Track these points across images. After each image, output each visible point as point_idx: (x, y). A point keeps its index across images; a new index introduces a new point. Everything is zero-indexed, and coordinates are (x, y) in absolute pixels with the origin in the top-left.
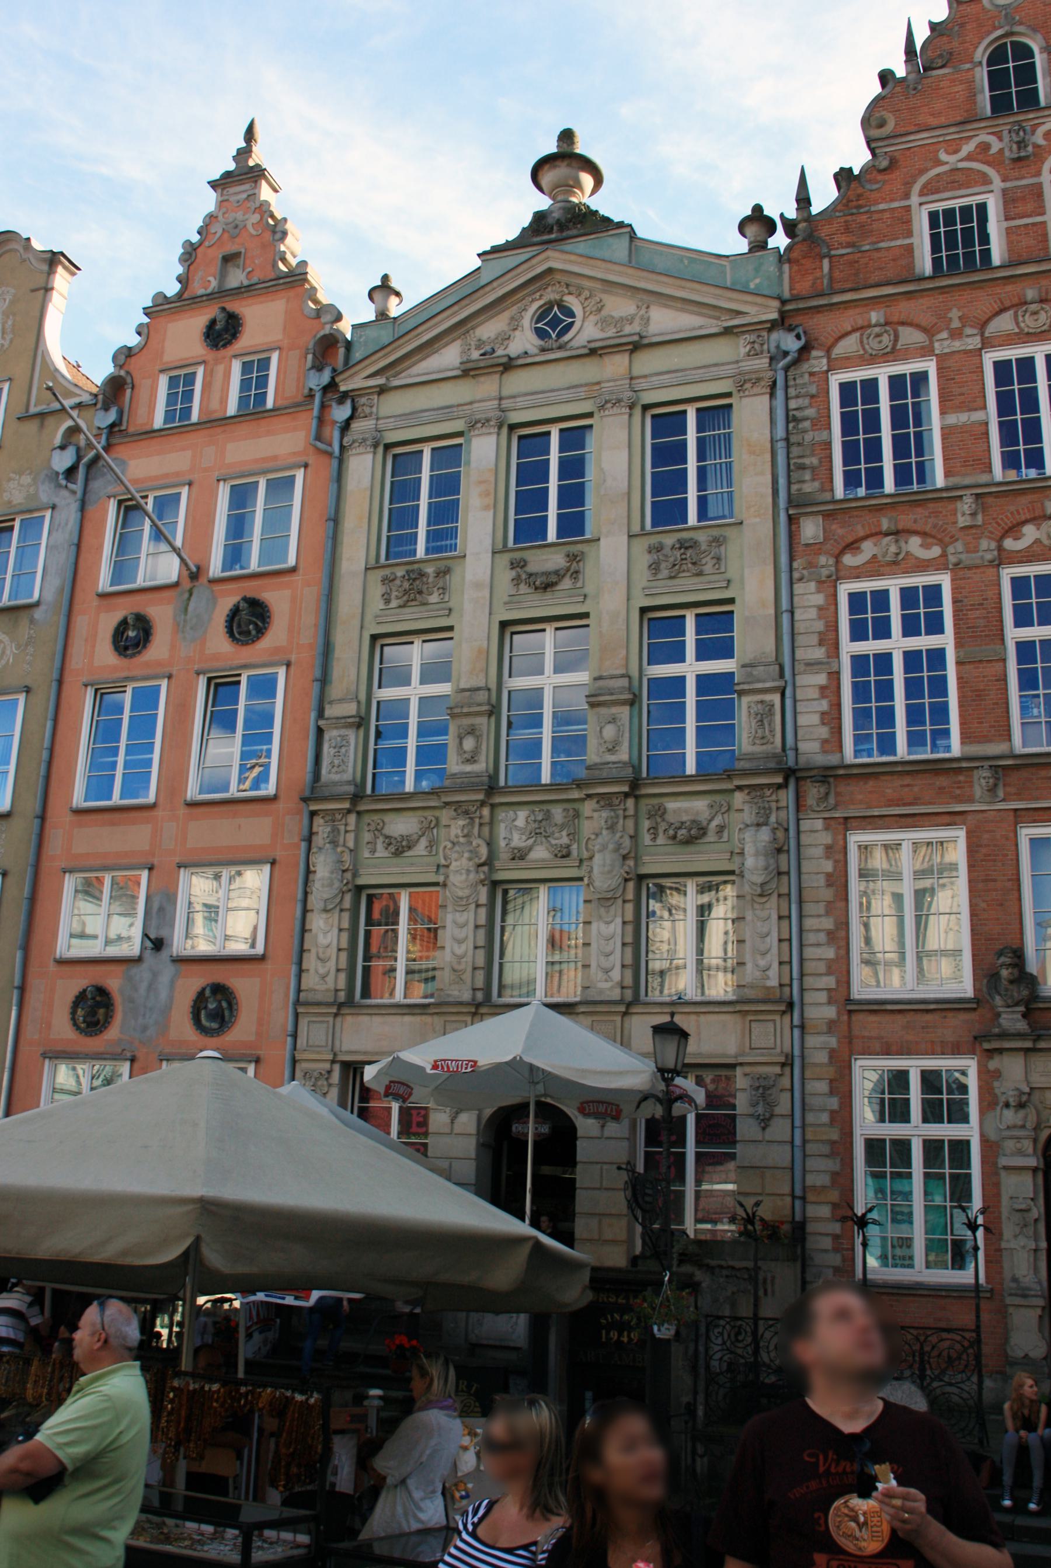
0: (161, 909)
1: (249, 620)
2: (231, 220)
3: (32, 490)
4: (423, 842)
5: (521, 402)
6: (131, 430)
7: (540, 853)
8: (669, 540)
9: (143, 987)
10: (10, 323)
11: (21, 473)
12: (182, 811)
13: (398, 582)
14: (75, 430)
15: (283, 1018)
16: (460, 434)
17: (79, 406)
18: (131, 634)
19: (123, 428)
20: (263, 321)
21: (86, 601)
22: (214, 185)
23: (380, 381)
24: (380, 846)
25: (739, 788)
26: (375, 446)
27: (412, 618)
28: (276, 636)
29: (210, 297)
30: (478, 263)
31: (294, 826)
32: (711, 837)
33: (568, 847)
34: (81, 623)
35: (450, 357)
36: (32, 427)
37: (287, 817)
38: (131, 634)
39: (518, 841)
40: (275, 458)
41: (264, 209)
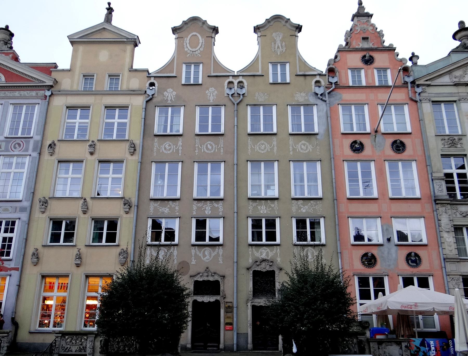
0: (387, 230)
1: (399, 146)
2: (362, 27)
3: (306, 98)
6: (341, 85)
9: (386, 253)
10: (284, 44)
11: (301, 92)
12: (388, 200)
13: (446, 140)
15: (436, 263)
16: (455, 101)
17: (320, 75)
18: (357, 146)
19: (338, 83)
20: (380, 59)
24: (458, 214)
27: (453, 151)
28: (409, 151)
29: (363, 50)
31: (428, 207)
34: (337, 141)
35: (446, 79)
36: (302, 78)
37: (426, 204)
38: (357, 146)
41: (373, 25)
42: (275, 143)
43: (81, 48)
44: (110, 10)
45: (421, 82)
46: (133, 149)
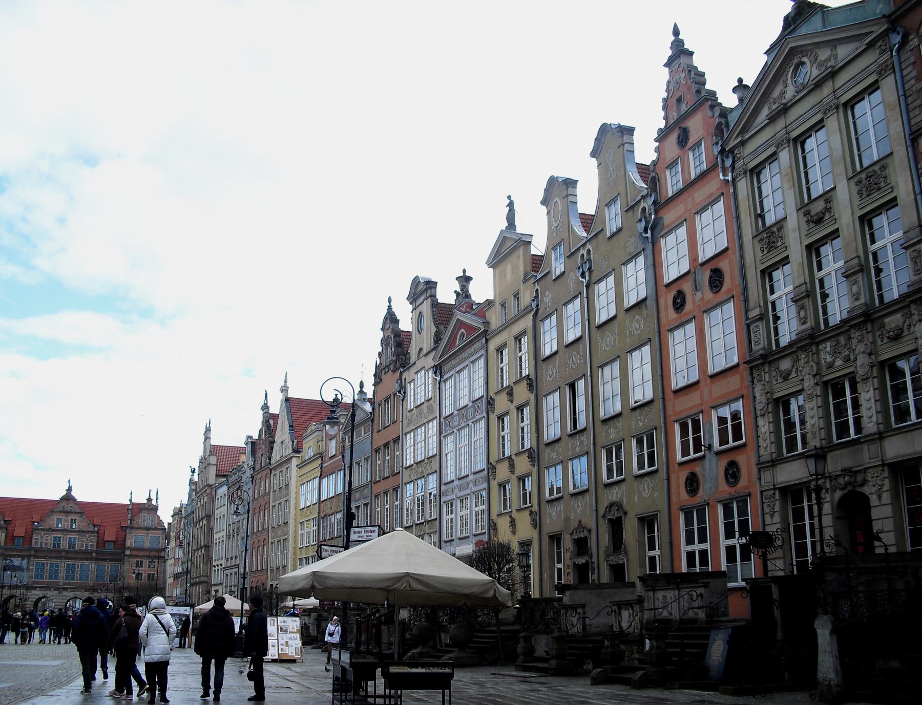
4: (794, 370)
5: (794, 125)
7: (839, 362)
8: (863, 176)
14: (644, 209)
20: (697, 126)
21: (662, 290)
22: (666, 65)
23: (739, 139)
25: (911, 302)
26: (745, 173)
30: (765, 58)
32: (906, 333)
33: (848, 356)
34: (662, 301)
35: (765, 112)
36: (631, 213)
39: (829, 359)
40: (712, 194)
42: (616, 331)
43: (497, 271)
44: (511, 205)
45: (732, 143)
46: (530, 386)
